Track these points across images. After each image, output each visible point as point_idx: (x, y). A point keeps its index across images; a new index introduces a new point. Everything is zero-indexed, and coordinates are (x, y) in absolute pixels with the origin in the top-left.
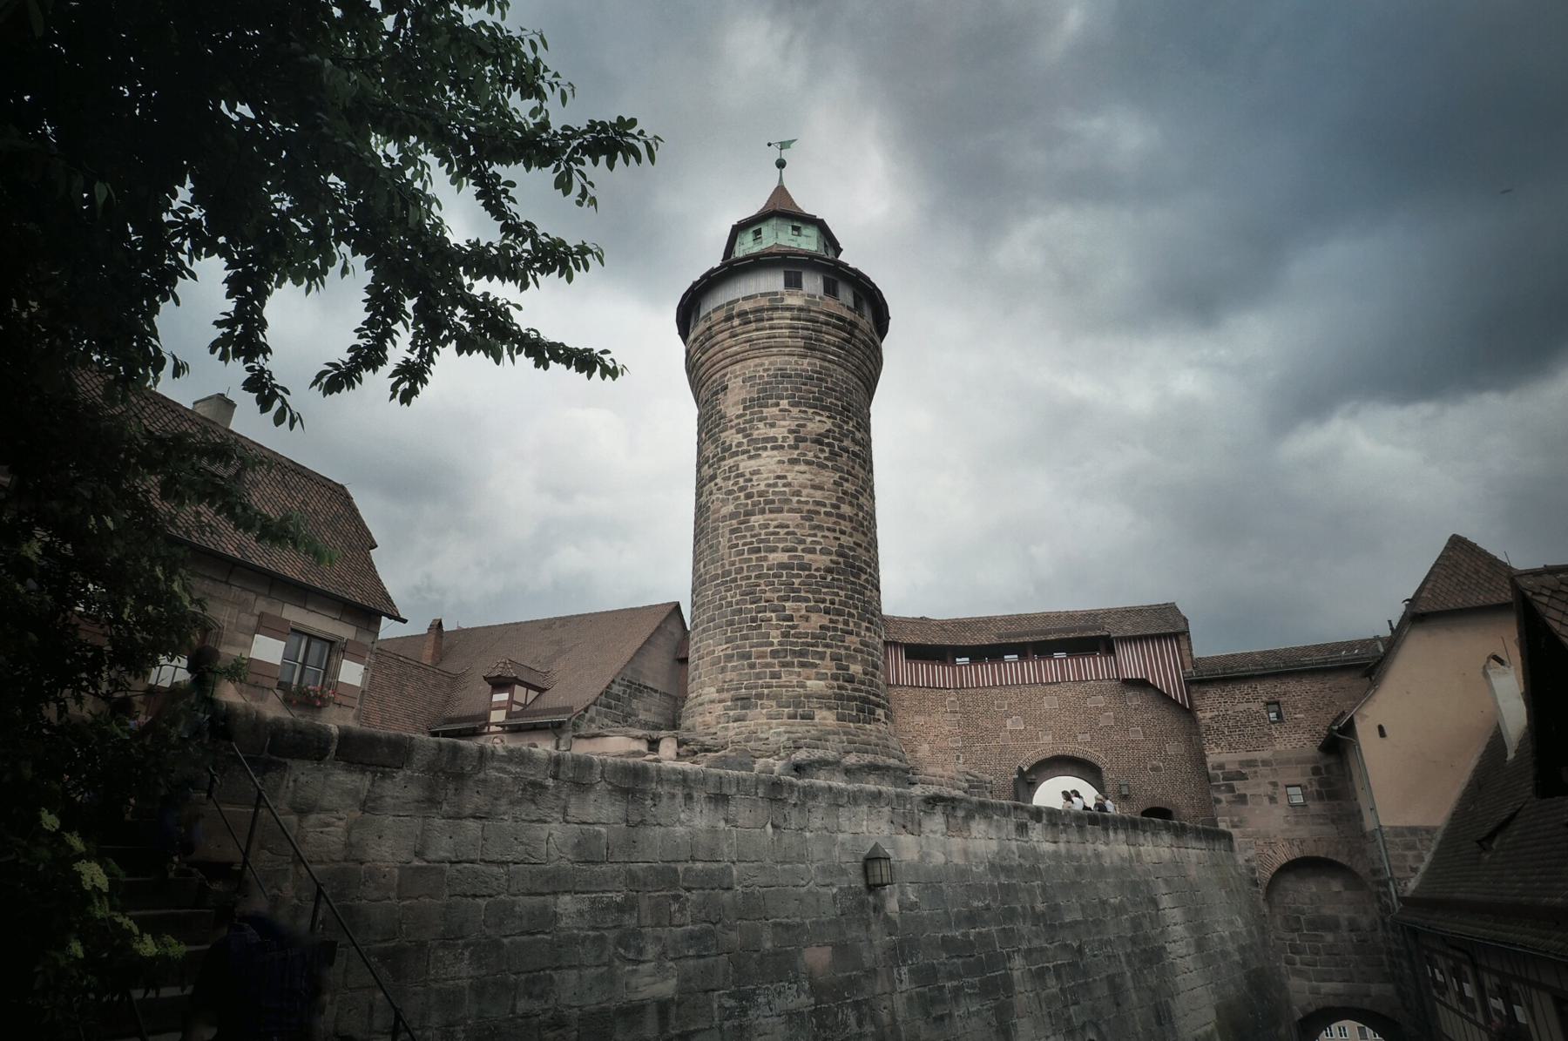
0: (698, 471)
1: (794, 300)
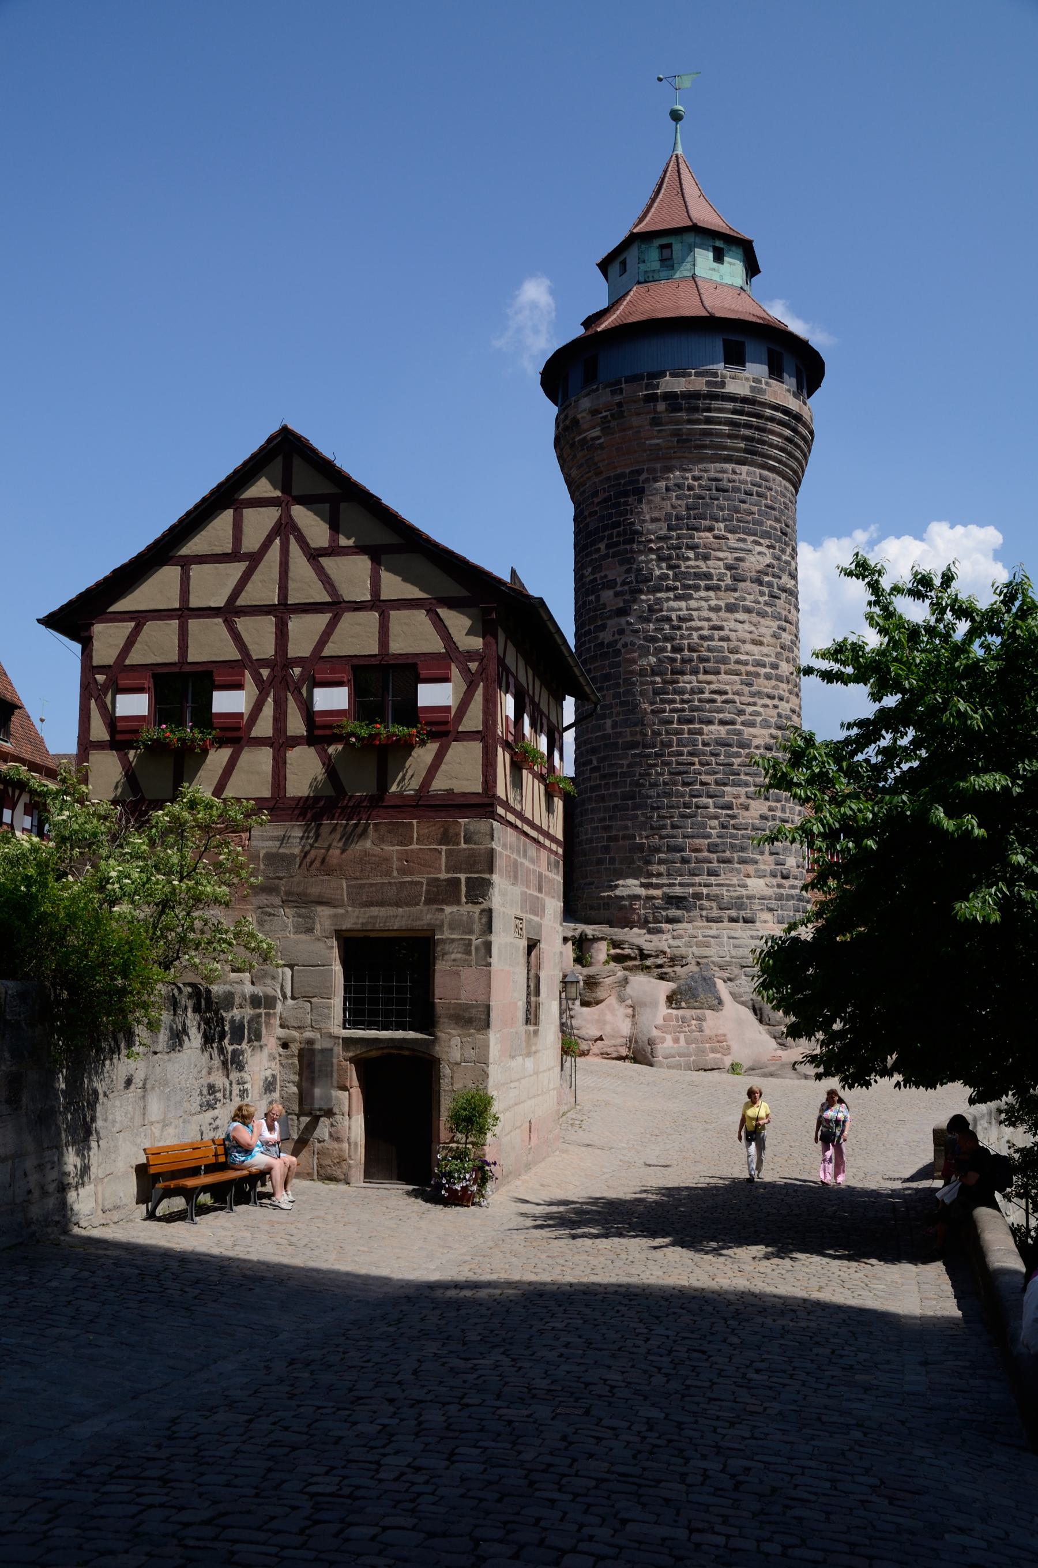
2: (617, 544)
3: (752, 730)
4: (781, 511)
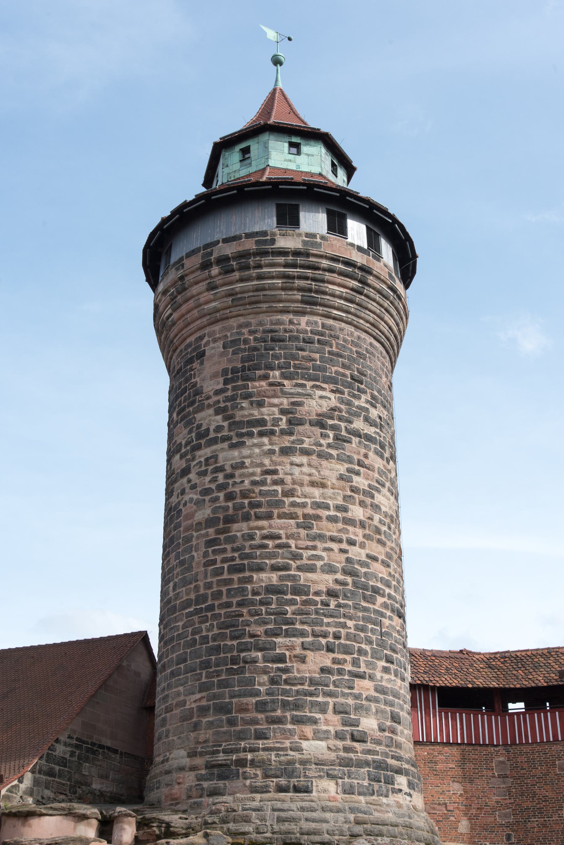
0: (169, 461)
1: (288, 242)
2: (183, 409)
3: (309, 575)
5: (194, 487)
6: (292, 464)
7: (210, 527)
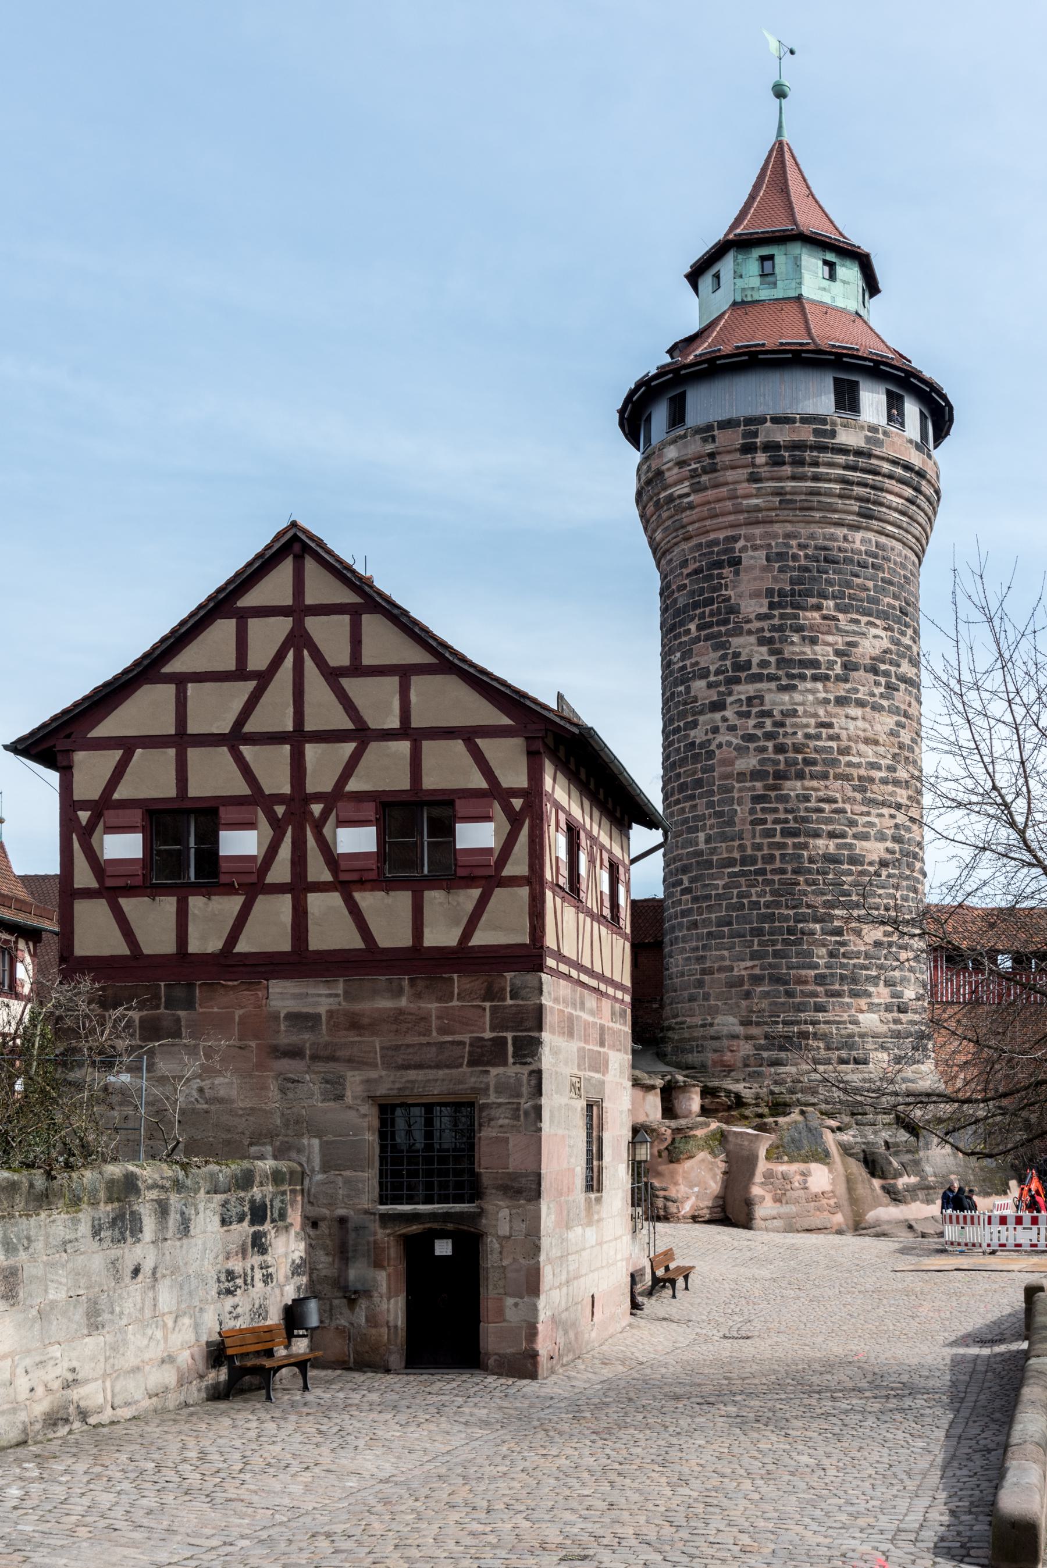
2: (710, 625)
4: (901, 587)
5: (732, 728)
6: (847, 717)
7: (756, 780)
